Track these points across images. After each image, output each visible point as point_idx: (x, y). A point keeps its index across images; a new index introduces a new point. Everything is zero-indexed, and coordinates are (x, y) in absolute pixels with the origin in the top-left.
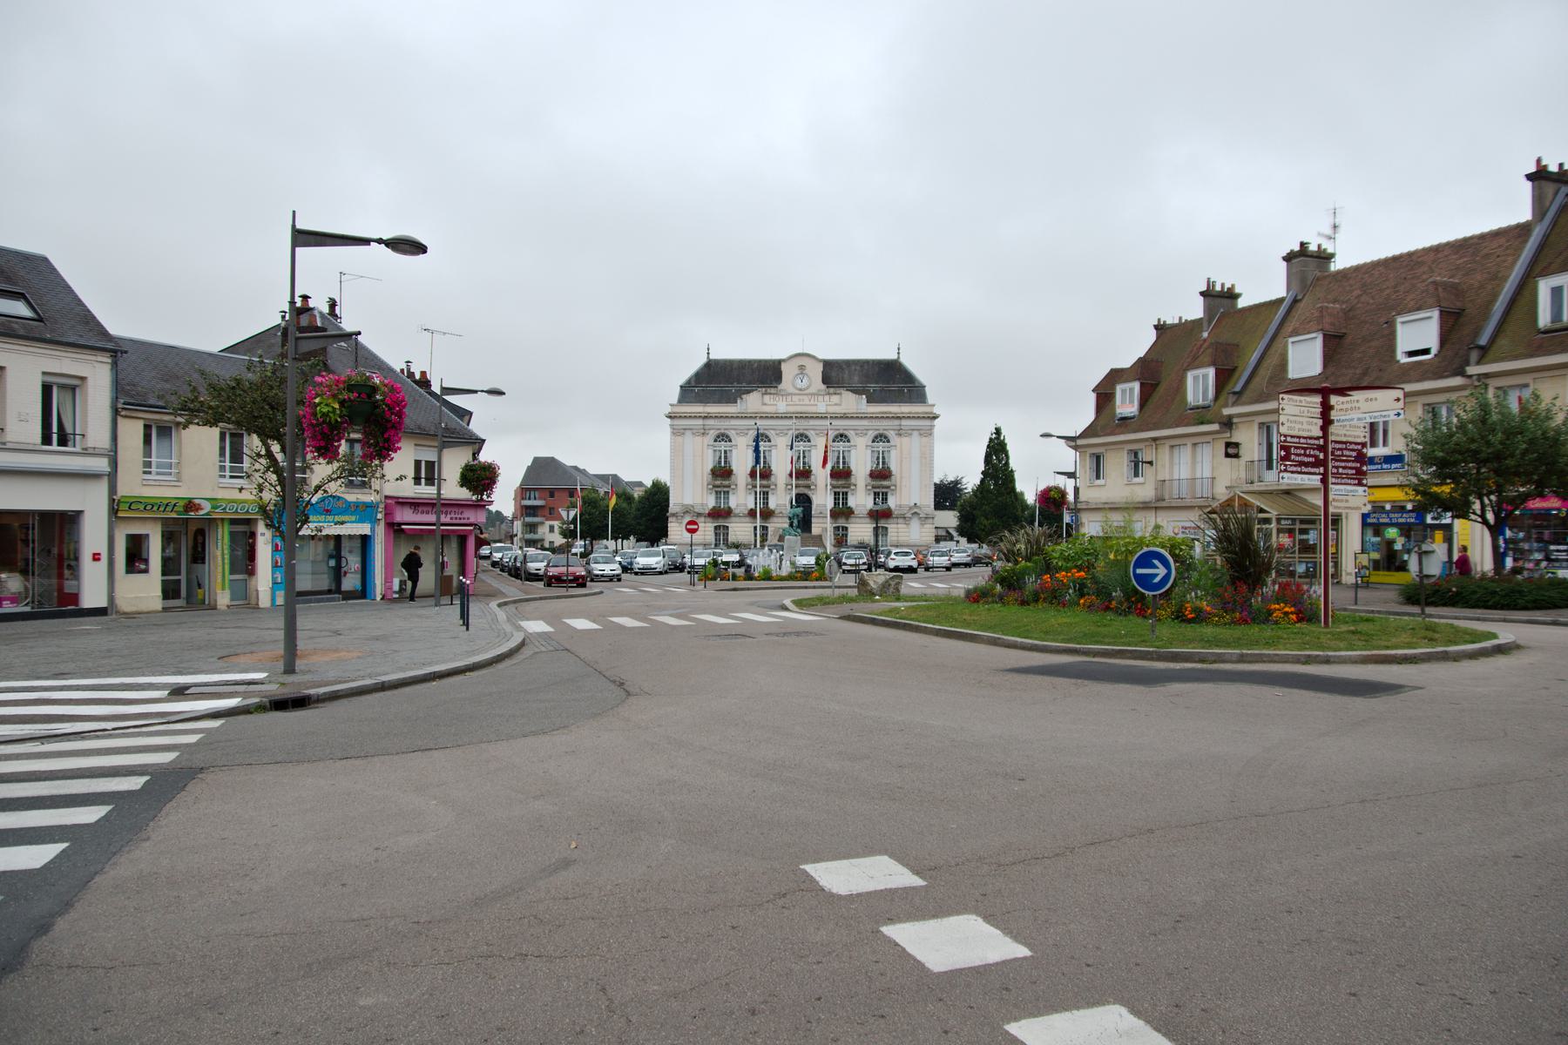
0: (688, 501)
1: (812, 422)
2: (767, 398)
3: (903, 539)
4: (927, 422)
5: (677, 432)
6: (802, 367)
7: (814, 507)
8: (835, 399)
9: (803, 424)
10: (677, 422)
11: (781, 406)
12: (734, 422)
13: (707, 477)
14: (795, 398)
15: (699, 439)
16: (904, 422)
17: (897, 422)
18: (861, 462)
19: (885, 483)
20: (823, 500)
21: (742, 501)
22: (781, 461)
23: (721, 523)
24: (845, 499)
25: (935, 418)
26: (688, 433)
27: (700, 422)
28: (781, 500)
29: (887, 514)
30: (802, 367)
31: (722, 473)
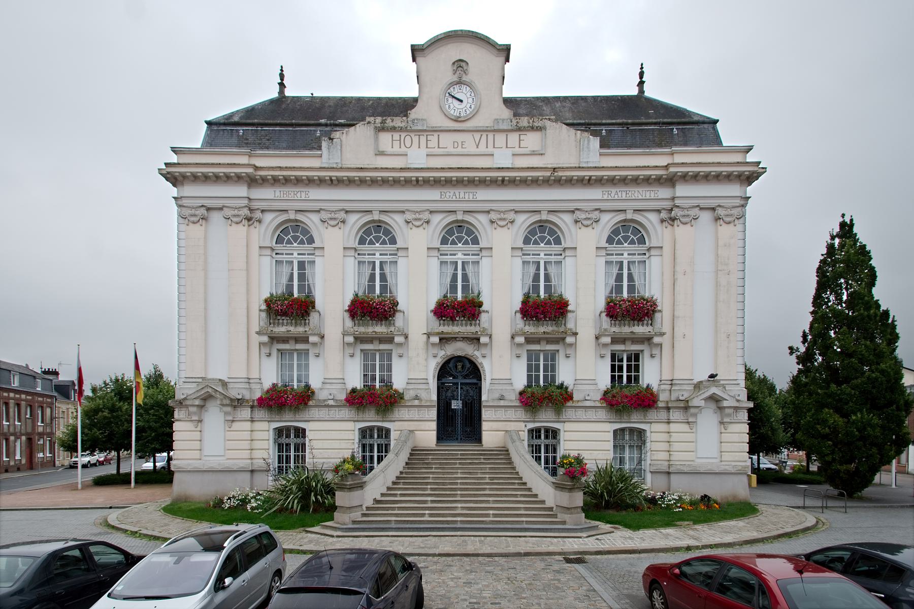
0: (218, 372)
1: (483, 194)
2: (385, 139)
3: (681, 457)
4: (734, 190)
5: (194, 215)
6: (460, 65)
7: (486, 385)
8: (532, 140)
9: (460, 199)
10: (190, 190)
11: (417, 155)
12: (316, 194)
13: (258, 319)
14: (447, 140)
15: (241, 230)
16: (682, 190)
17: (664, 193)
18: (585, 287)
19: (640, 329)
20: (504, 370)
21: (335, 374)
22: (417, 290)
23: (288, 420)
24: (551, 368)
25: (750, 178)
26: (216, 217)
27: (241, 191)
28: (415, 370)
29: (646, 401)
30: (460, 65)
31: (291, 309)
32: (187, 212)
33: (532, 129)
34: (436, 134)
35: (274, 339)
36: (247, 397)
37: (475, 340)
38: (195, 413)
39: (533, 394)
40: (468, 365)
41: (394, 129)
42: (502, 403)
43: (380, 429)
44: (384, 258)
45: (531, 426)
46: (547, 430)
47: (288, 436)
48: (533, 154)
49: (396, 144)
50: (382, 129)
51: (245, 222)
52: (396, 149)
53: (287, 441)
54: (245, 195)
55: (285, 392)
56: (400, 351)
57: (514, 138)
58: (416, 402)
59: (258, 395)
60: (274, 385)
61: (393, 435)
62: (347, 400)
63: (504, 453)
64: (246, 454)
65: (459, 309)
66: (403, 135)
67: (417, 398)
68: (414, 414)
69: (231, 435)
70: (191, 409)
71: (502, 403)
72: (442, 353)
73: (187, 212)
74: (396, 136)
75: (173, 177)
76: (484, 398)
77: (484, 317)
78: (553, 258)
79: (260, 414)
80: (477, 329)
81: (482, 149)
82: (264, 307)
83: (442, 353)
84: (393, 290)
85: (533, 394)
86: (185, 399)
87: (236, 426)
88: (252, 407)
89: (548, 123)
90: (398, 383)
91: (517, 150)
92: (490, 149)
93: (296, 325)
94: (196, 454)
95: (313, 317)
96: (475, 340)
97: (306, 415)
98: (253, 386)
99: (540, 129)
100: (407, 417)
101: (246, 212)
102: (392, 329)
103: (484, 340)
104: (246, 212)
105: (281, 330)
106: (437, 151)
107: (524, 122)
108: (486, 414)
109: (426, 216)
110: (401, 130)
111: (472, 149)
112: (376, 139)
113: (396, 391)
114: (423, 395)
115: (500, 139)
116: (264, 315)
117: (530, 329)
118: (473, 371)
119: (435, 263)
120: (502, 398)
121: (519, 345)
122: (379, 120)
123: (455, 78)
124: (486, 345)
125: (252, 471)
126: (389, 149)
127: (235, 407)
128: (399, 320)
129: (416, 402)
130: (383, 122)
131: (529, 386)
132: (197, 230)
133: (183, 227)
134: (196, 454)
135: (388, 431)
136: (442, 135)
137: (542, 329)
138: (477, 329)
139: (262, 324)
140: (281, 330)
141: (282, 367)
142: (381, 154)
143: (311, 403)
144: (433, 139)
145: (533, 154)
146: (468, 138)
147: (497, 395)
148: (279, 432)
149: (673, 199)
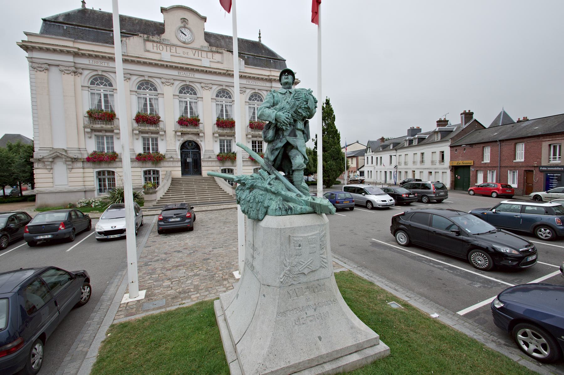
0: (60, 144)
2: (149, 45)
6: (184, 20)
7: (203, 153)
8: (217, 57)
9: (189, 76)
10: (36, 55)
11: (166, 55)
13: (83, 120)
14: (180, 50)
15: (70, 78)
17: (268, 84)
20: (210, 147)
22: (169, 111)
23: (104, 167)
24: (229, 146)
26: (54, 70)
27: (70, 58)
28: (170, 145)
31: (102, 117)
32: (36, 65)
33: (218, 52)
34: (175, 47)
35: (93, 130)
36: (80, 156)
37: (197, 134)
38: (48, 165)
39: (223, 156)
40: (194, 144)
41: (153, 41)
42: (210, 159)
43: (154, 171)
44: (151, 97)
45: (222, 168)
46: (229, 170)
47: (104, 175)
48: (218, 62)
49: (155, 48)
50: (148, 40)
51: (73, 74)
52: (155, 50)
53: (104, 177)
54: (72, 61)
55: (103, 155)
56: (162, 138)
57: (210, 55)
58: (172, 159)
59: (86, 156)
60: (95, 152)
61: (161, 173)
62: (137, 158)
63: (212, 177)
64: (81, 184)
65: (189, 122)
66: (158, 45)
67: (172, 157)
68: (170, 164)
69: (70, 175)
70: (46, 163)
71: (210, 159)
72: (182, 139)
73: (36, 65)
74: (155, 44)
75: (25, 47)
76: (202, 157)
77: (201, 125)
78: (228, 104)
79: (87, 165)
80: (198, 130)
81: (196, 56)
82: (87, 115)
83: (182, 139)
84: (157, 111)
85: (223, 156)
86: (43, 158)
87: (74, 171)
88: (83, 162)
89: (224, 51)
90: (162, 150)
91: (211, 60)
92: (200, 58)
93: (106, 124)
94: (51, 185)
95: (115, 121)
96: (197, 134)
97: (115, 165)
98: (83, 152)
99: (221, 53)
100: (167, 165)
101: (74, 69)
102: (158, 128)
103: (201, 135)
104: (74, 69)
105: (98, 126)
106: (175, 54)
107: (214, 49)
108: (203, 164)
109: (172, 81)
110: (157, 42)
111: (192, 56)
112: (145, 45)
113: (161, 155)
114: (174, 156)
115: (204, 54)
116: (87, 119)
117: (221, 131)
118: (197, 147)
119: (177, 101)
120: (210, 158)
121: (216, 137)
122: (146, 36)
123: (182, 25)
124: (202, 137)
125: (85, 191)
126: (152, 50)
127: (73, 162)
128: (161, 125)
129: (172, 159)
130: (148, 37)
131: (221, 153)
132: (42, 75)
133: (33, 72)
134: (51, 185)
135: (158, 172)
136: (177, 48)
137: (225, 131)
138: (198, 130)
139: (86, 123)
140: (98, 126)
141: (99, 144)
142: (148, 51)
143: (117, 160)
144: (173, 49)
145: (218, 62)
146: (190, 51)
147: (208, 157)
148: (99, 173)
149: (271, 87)
